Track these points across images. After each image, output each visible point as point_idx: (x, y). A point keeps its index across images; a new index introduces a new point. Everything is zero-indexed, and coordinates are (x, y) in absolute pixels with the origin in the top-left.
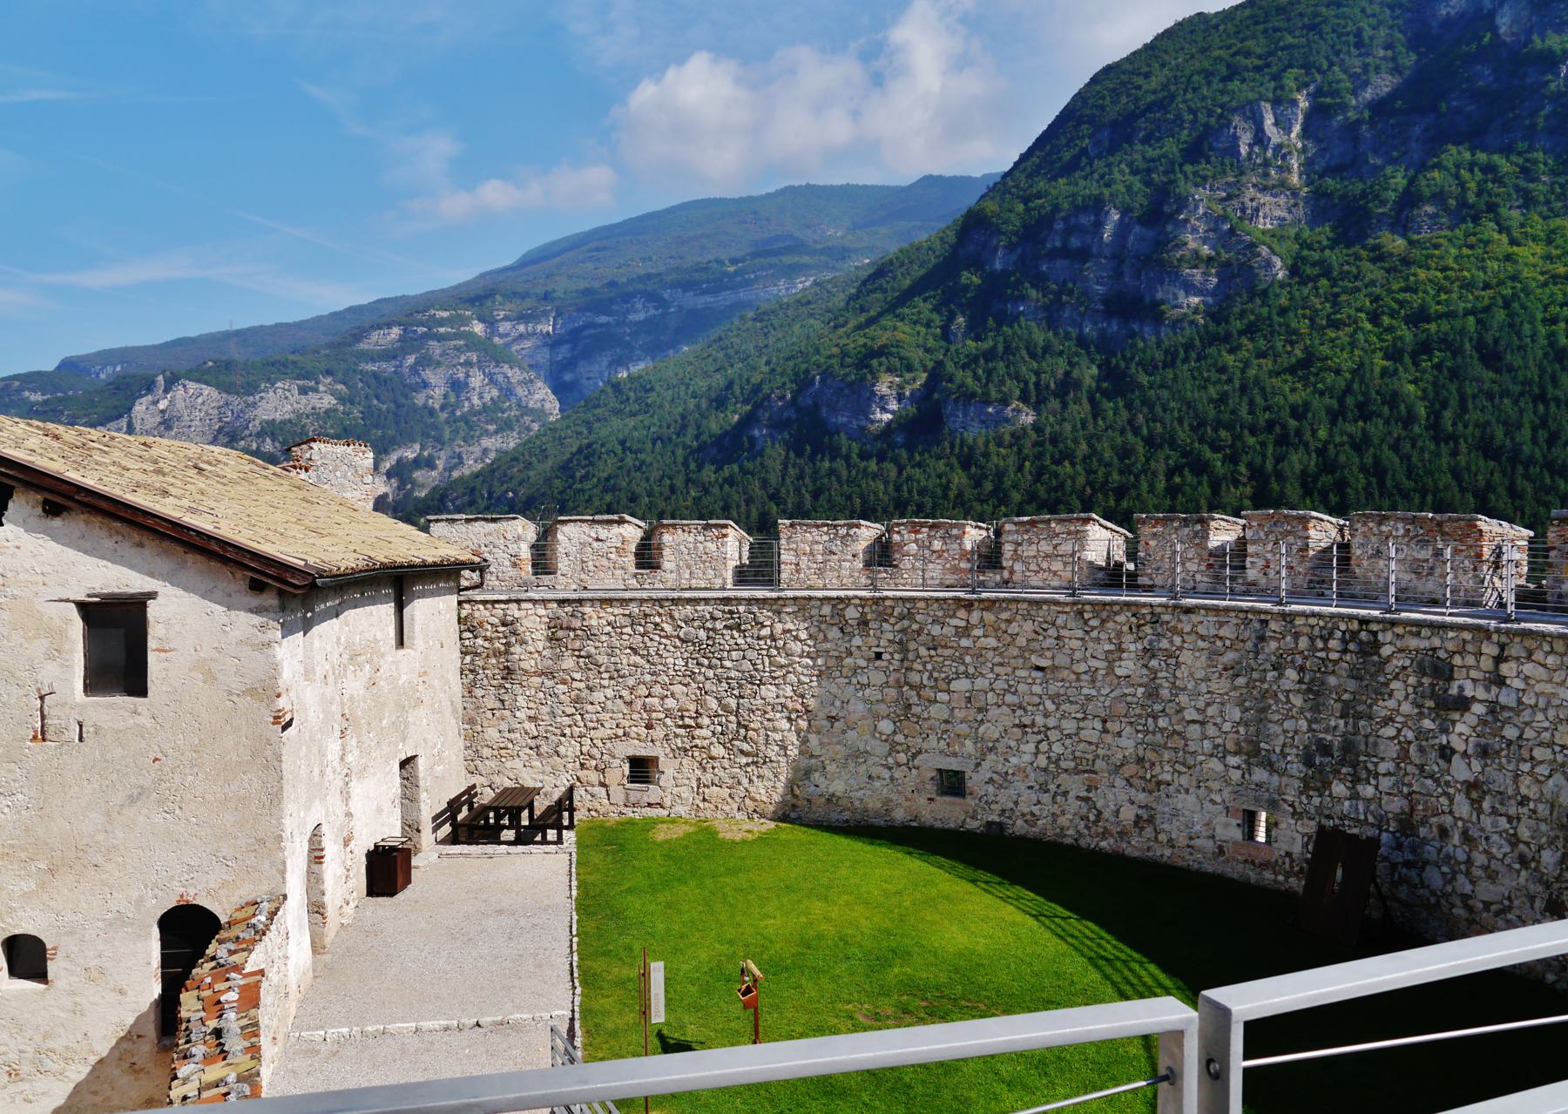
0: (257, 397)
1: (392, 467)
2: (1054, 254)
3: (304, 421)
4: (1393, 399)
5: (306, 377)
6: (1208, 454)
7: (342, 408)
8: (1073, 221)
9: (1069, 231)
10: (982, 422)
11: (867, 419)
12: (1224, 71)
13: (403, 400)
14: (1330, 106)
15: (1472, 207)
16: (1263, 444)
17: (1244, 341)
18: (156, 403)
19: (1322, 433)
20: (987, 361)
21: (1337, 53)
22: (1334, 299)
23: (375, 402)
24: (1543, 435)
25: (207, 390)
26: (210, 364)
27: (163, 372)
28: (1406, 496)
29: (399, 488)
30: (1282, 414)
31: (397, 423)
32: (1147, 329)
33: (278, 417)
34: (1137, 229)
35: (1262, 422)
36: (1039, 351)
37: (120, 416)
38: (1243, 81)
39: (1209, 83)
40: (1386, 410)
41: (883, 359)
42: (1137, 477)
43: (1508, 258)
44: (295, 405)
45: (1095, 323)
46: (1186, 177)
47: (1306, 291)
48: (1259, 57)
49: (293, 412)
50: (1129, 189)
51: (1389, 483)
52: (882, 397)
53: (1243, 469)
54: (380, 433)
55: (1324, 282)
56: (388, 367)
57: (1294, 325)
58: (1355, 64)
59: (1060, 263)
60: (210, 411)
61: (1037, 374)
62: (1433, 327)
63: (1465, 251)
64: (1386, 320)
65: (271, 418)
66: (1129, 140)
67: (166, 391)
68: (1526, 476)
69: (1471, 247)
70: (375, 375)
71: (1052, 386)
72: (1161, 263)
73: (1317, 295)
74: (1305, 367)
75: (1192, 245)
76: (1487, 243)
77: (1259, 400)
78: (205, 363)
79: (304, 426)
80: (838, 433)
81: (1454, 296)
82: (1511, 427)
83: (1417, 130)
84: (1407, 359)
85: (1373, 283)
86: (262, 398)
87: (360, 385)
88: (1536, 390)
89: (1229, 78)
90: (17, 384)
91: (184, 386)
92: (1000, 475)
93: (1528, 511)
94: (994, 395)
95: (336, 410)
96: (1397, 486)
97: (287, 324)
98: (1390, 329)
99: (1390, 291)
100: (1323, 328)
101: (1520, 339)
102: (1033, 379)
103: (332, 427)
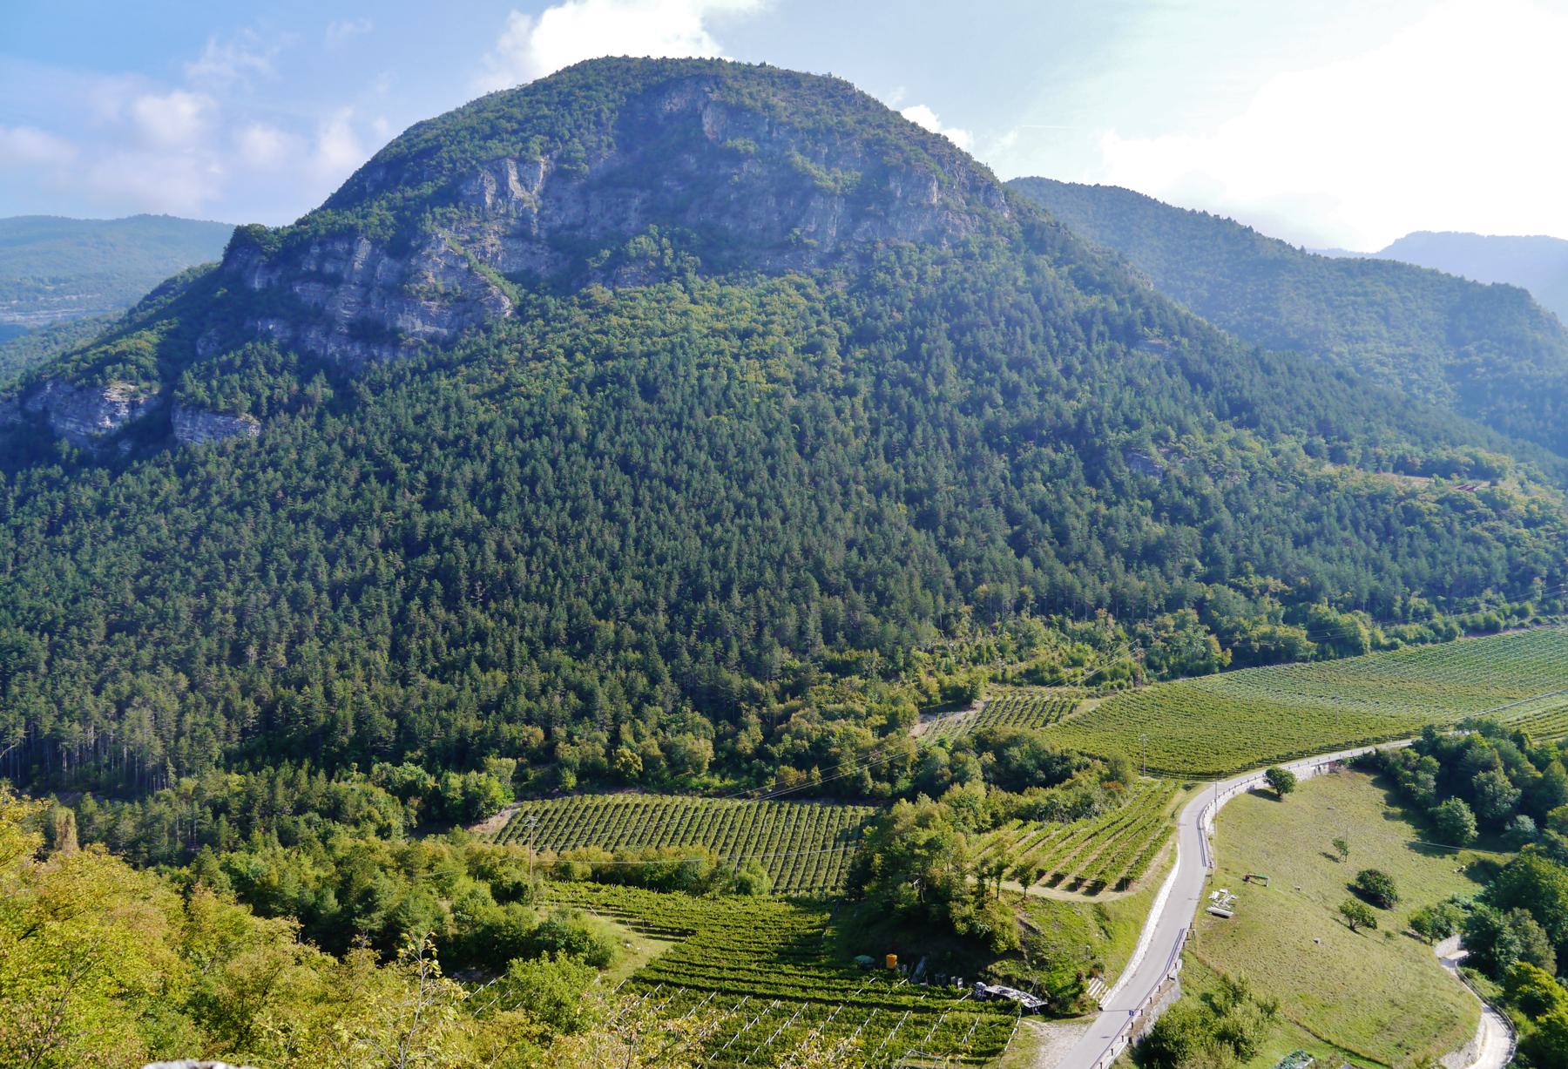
2: (310, 277)
4: (561, 421)
6: (397, 463)
8: (329, 248)
9: (323, 257)
10: (211, 432)
11: (95, 426)
12: (487, 129)
14: (567, 171)
15: (667, 269)
16: (446, 457)
17: (463, 368)
19: (499, 448)
20: (223, 373)
21: (579, 127)
22: (542, 337)
24: (671, 453)
28: (550, 503)
30: (470, 430)
32: (385, 354)
34: (386, 260)
35: (451, 436)
36: (277, 367)
38: (502, 141)
39: (472, 139)
40: (555, 430)
41: (120, 366)
42: (327, 482)
43: (685, 313)
45: (339, 346)
46: (434, 219)
47: (523, 328)
48: (519, 123)
50: (382, 222)
51: (539, 491)
52: (113, 404)
53: (422, 477)
55: (540, 322)
57: (505, 356)
58: (592, 140)
59: (314, 287)
61: (271, 388)
62: (610, 364)
63: (654, 304)
64: (579, 356)
66: (397, 181)
68: (650, 489)
69: (658, 302)
71: (286, 400)
72: (401, 293)
73: (532, 333)
74: (499, 394)
75: (431, 280)
76: (670, 299)
77: (454, 418)
80: (60, 439)
81: (636, 340)
82: (647, 446)
83: (637, 202)
84: (583, 387)
85: (576, 325)
88: (675, 419)
89: (491, 137)
92: (209, 481)
93: (642, 516)
94: (222, 405)
96: (546, 494)
98: (581, 364)
99: (587, 332)
100: (529, 360)
101: (675, 377)
102: (267, 393)
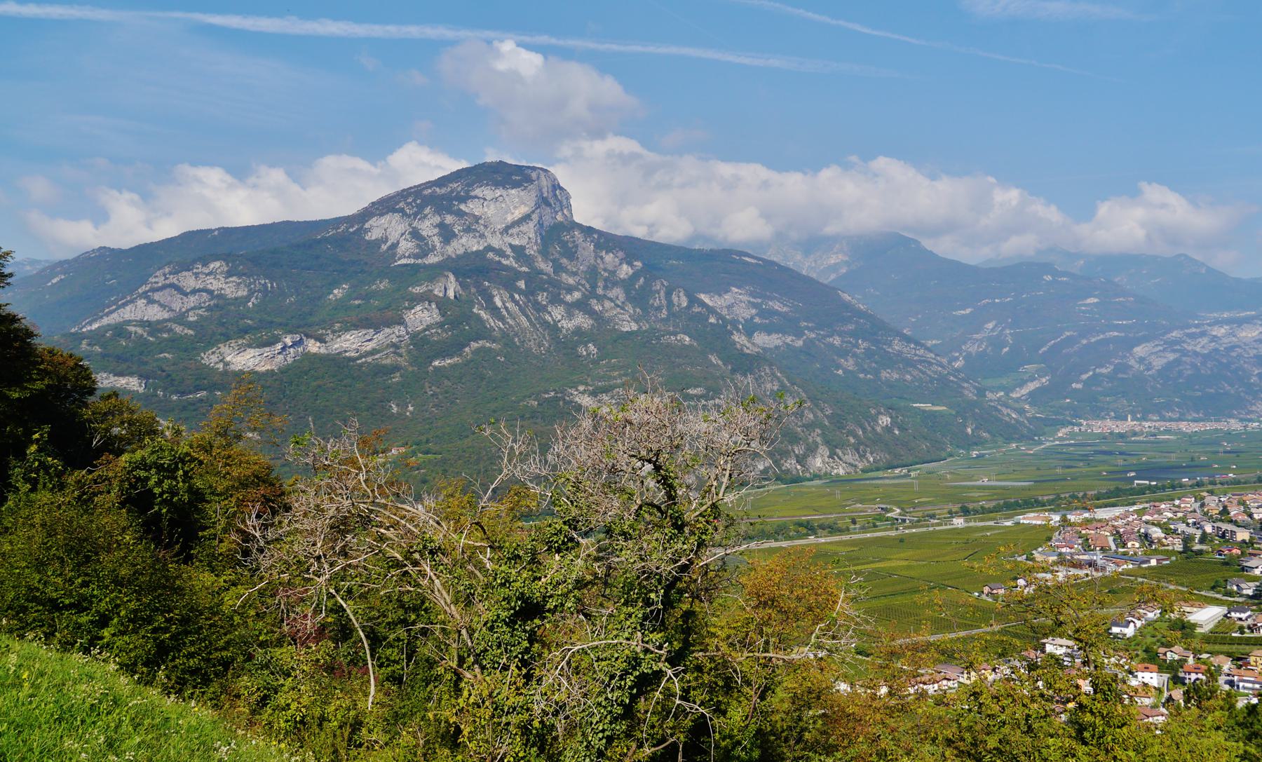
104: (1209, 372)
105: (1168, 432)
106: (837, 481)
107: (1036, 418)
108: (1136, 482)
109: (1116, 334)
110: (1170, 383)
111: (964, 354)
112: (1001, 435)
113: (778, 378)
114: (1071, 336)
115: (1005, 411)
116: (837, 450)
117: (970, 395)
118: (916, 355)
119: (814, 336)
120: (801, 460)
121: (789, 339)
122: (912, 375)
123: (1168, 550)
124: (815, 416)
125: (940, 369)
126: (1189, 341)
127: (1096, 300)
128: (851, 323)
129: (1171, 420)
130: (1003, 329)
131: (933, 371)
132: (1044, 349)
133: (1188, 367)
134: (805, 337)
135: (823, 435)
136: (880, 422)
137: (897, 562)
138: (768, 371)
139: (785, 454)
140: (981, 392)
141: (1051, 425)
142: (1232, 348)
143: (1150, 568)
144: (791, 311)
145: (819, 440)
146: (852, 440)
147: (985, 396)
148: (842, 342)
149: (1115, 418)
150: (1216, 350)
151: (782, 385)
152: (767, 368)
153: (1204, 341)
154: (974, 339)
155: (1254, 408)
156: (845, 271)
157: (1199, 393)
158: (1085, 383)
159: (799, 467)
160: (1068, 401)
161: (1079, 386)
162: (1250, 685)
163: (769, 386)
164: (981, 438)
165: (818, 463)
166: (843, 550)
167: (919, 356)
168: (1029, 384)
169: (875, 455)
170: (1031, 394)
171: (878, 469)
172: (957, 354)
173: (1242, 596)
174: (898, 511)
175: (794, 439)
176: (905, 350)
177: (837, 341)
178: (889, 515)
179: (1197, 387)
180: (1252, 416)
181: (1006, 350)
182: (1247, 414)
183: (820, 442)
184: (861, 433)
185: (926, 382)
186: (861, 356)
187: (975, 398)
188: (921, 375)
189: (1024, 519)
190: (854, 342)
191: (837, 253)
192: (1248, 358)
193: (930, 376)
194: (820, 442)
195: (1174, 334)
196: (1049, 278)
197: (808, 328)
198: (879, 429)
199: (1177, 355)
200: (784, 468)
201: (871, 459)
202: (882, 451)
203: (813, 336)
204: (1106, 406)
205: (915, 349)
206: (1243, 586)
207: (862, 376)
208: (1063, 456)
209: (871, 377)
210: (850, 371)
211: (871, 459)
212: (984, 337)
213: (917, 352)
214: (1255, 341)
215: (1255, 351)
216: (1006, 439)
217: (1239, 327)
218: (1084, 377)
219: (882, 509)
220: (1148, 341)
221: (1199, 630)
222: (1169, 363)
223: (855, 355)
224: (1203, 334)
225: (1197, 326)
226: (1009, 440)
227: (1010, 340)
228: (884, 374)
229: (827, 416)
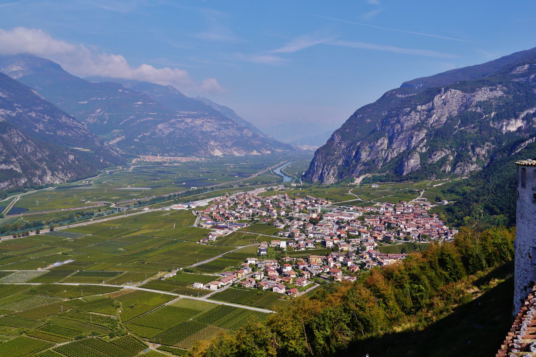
0: (475, 93)
1: (524, 116)
3: (491, 101)
5: (492, 85)
7: (505, 96)
13: (529, 92)
18: (441, 97)
23: (518, 93)
25: (458, 92)
26: (458, 82)
27: (444, 86)
29: (527, 124)
31: (527, 100)
33: (482, 100)
37: (429, 102)
44: (488, 95)
49: (488, 98)
54: (520, 104)
56: (523, 80)
60: (459, 99)
65: (480, 100)
67: (445, 93)
70: (517, 82)
78: (456, 82)
79: (491, 103)
86: (477, 93)
87: (512, 87)
90: (394, 92)
91: (451, 91)
95: (503, 96)
97: (479, 65)
103: (502, 103)
104: (185, 137)
105: (175, 162)
106: (59, 188)
107: (123, 154)
108: (192, 188)
109: (151, 118)
110: (171, 140)
111: (87, 123)
112: (113, 163)
113: (21, 136)
114: (133, 118)
115: (112, 151)
116: (56, 173)
117: (98, 144)
118: (73, 124)
119: (21, 111)
120: (41, 177)
121: (8, 112)
122: (71, 133)
123: (244, 220)
124: (42, 155)
125: (84, 131)
126: (178, 124)
127: (141, 103)
128: (41, 106)
129: (172, 156)
130: (104, 113)
131: (81, 132)
132: (122, 123)
133: (178, 134)
134: (17, 112)
135: (47, 165)
136: (69, 158)
137: (145, 230)
138: (15, 132)
139: (34, 175)
140: (102, 142)
141: (128, 158)
142: (192, 127)
143: (245, 228)
144: (8, 98)
145: (46, 167)
146: (60, 167)
147: (104, 145)
148: (37, 115)
149: (152, 154)
150: (187, 128)
151: (23, 139)
152: (14, 130)
153: (183, 124)
154: (91, 116)
155: (200, 152)
156: (21, 76)
157: (182, 145)
158: (139, 139)
159: (40, 181)
160: (133, 147)
161: (137, 140)
162: (316, 267)
163: (16, 140)
164: (107, 164)
165: (48, 179)
166: (117, 226)
167: (75, 125)
168: (117, 138)
169: (71, 174)
170: (117, 143)
171: (74, 181)
172: (84, 123)
173: (285, 237)
174: (114, 204)
175: (37, 168)
176: (68, 122)
177: (33, 115)
178: (111, 206)
179: (181, 143)
180: (200, 155)
181: (106, 122)
182: (198, 154)
183: (46, 168)
184: (63, 163)
185: (79, 138)
186: (46, 123)
187: (100, 145)
188: (76, 133)
189: (174, 207)
190: (42, 116)
191: (17, 65)
192: (198, 132)
193: (79, 134)
194: (46, 168)
195: (172, 121)
196: (121, 91)
197: (18, 107)
198: (70, 161)
199: (174, 129)
200: (34, 182)
201: (70, 176)
202: (73, 172)
203: (21, 111)
204: (148, 150)
205: (73, 121)
206: (285, 233)
207: (47, 133)
208: (149, 174)
209: (52, 134)
210: (42, 130)
211: (70, 176)
212: (95, 116)
213: (74, 123)
214: (200, 125)
215: (200, 129)
216: (115, 164)
217: (195, 119)
218: (139, 136)
219: (104, 203)
220: (163, 123)
221: (285, 250)
222: (170, 132)
223: (43, 122)
224: (183, 121)
225: (181, 118)
226: (116, 165)
227: (107, 117)
228: (59, 133)
229: (47, 155)
